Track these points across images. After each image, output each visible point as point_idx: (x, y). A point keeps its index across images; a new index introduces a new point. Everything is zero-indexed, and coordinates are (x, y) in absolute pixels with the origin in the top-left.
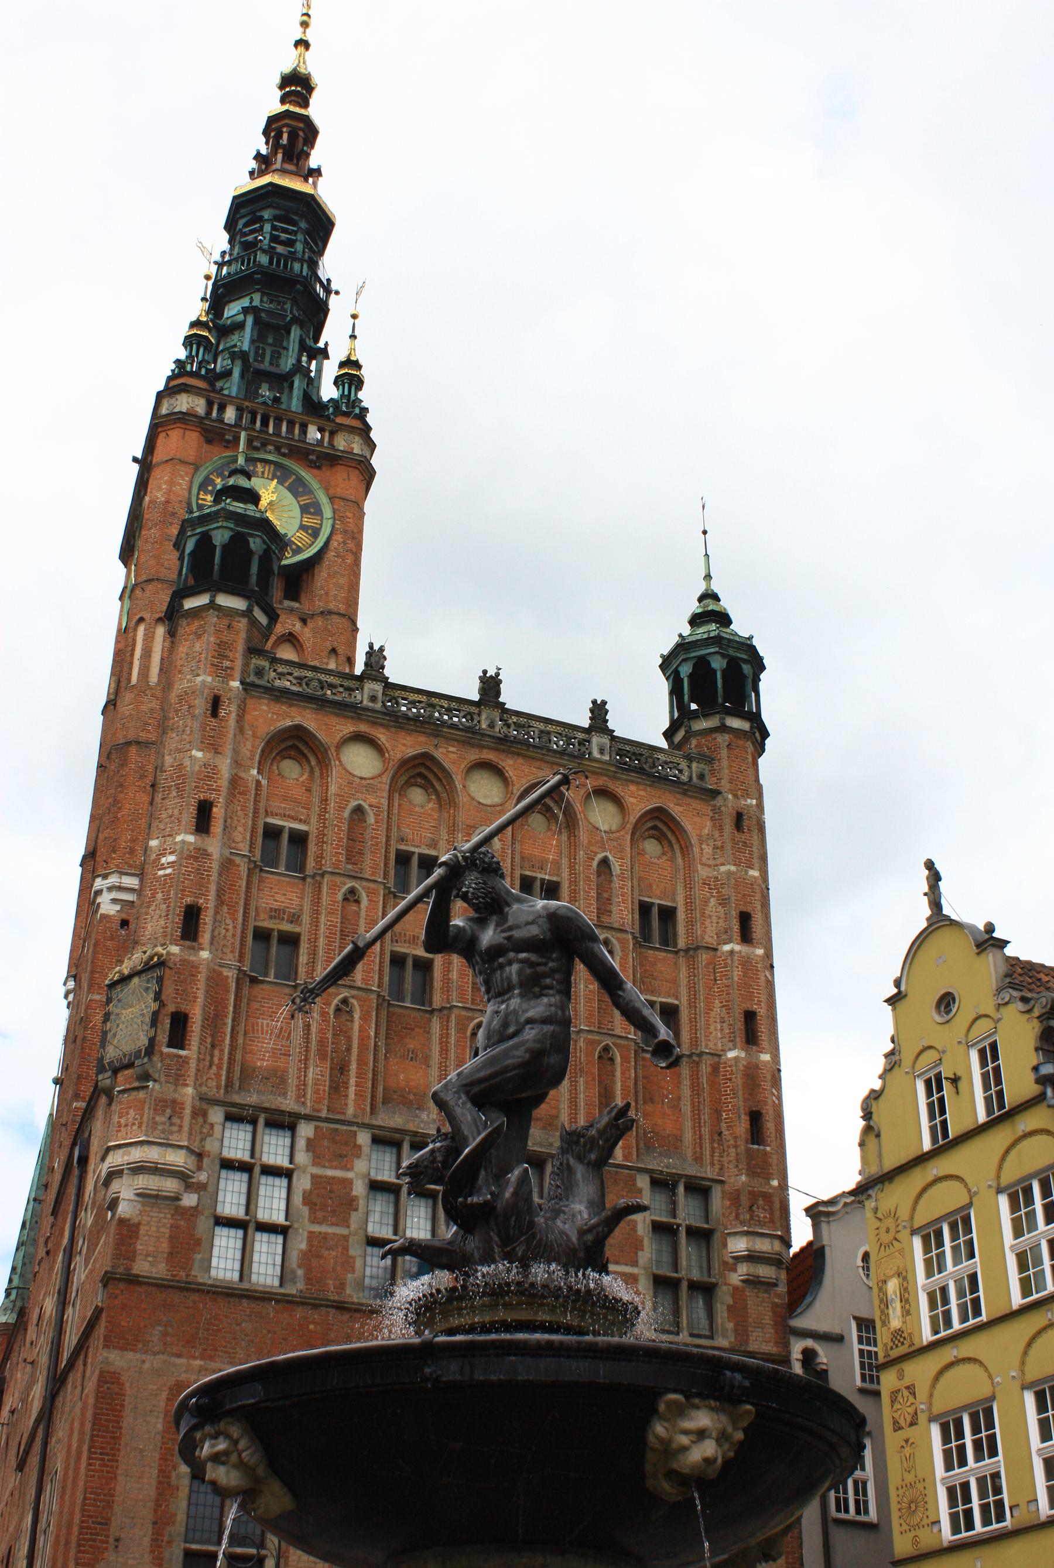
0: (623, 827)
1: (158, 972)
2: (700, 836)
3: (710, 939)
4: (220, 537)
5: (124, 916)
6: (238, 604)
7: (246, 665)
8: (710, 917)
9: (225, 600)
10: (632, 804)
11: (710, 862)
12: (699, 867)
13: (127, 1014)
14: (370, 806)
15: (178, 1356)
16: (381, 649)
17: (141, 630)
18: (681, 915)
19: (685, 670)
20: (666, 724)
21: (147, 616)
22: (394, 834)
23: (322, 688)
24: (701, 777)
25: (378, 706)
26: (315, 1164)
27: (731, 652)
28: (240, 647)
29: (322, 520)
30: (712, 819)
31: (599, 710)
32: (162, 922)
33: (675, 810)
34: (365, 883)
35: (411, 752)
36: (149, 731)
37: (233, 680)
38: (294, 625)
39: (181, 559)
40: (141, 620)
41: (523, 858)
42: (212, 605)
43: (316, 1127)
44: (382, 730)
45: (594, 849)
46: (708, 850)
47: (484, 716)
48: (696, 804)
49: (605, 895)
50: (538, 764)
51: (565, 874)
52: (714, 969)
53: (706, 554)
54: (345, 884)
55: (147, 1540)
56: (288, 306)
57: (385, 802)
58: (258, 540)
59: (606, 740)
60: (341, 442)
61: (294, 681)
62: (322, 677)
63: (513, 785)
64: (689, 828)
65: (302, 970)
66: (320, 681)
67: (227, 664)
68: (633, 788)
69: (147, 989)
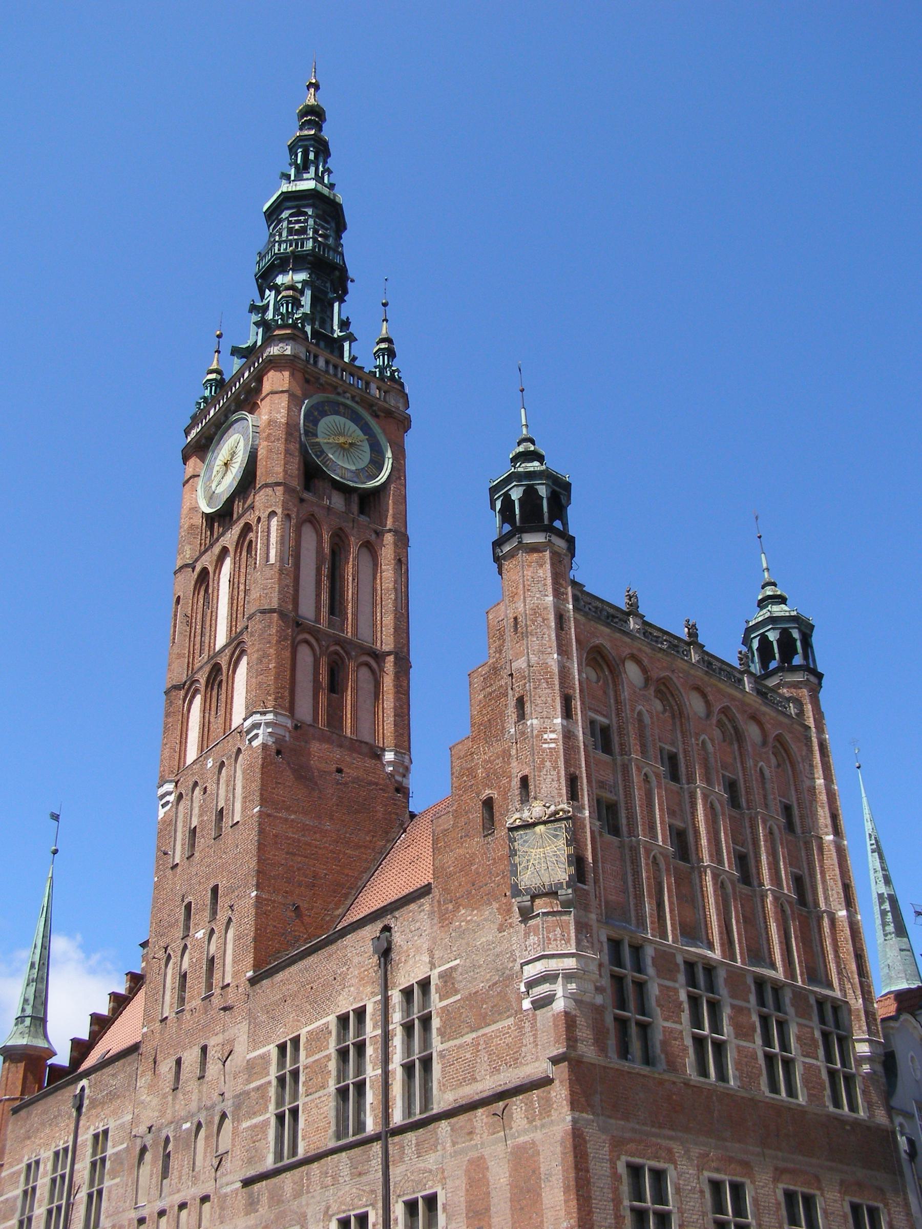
1: (563, 824)
12: (805, 779)
13: (535, 853)
15: (610, 1117)
18: (796, 811)
23: (608, 618)
26: (658, 977)
27: (803, 628)
32: (555, 784)
33: (788, 737)
34: (653, 769)
35: (663, 674)
40: (273, 513)
43: (655, 949)
51: (741, 774)
56: (328, 285)
60: (393, 401)
64: (796, 749)
65: (624, 829)
69: (556, 836)
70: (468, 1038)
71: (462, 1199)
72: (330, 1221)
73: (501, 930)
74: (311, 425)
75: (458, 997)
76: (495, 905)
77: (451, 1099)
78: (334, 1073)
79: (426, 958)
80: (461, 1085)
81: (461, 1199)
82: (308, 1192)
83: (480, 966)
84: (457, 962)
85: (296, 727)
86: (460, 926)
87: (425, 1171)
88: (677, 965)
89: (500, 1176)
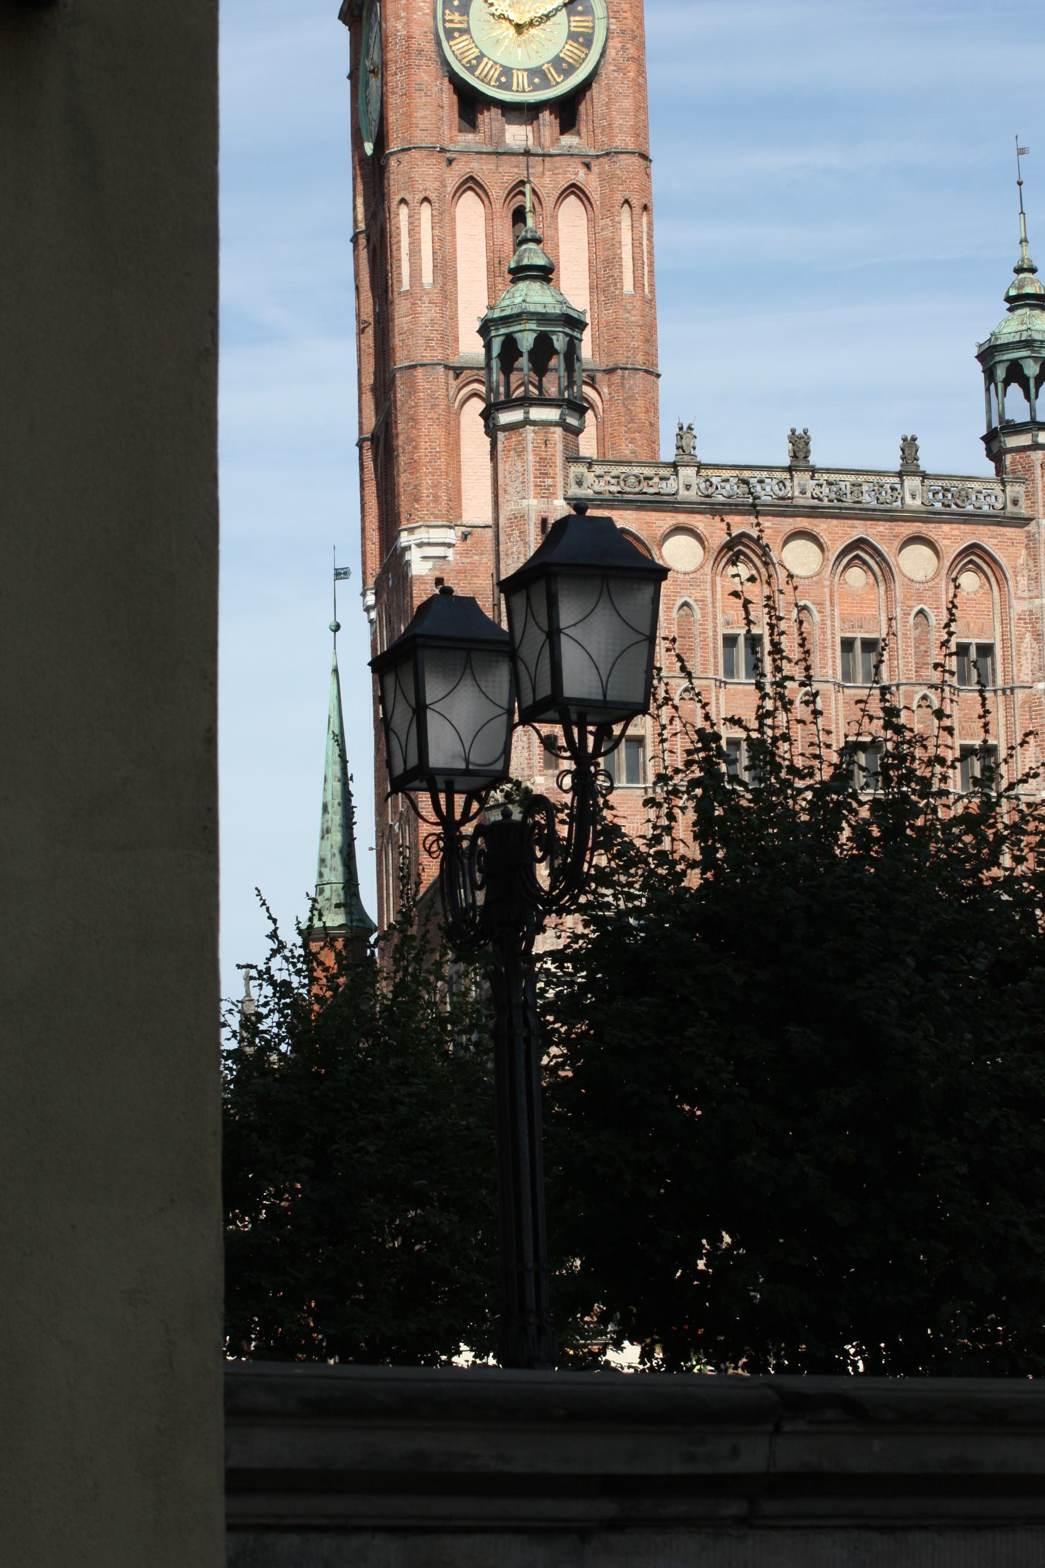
0: (937, 574)
2: (1015, 568)
3: (1025, 677)
4: (526, 341)
5: (438, 574)
6: (552, 414)
7: (566, 476)
8: (1026, 653)
9: (537, 413)
10: (946, 546)
11: (1026, 595)
14: (696, 601)
16: (690, 428)
17: (404, 211)
18: (998, 651)
19: (1001, 373)
20: (984, 432)
21: (408, 198)
22: (720, 620)
23: (639, 482)
24: (1015, 502)
25: (692, 495)
28: (559, 459)
29: (593, 22)
30: (1027, 547)
31: (909, 447)
32: (526, 754)
33: (989, 544)
36: (433, 349)
37: (556, 498)
38: (577, 174)
39: (488, 346)
40: (403, 201)
41: (843, 620)
42: (527, 422)
44: (698, 517)
45: (909, 603)
46: (1023, 581)
47: (796, 481)
48: (1009, 532)
49: (923, 648)
50: (850, 522)
52: (1030, 708)
53: (1022, 212)
54: (679, 686)
57: (709, 594)
58: (561, 335)
59: (917, 480)
61: (613, 481)
62: (636, 471)
63: (829, 550)
66: (636, 477)
67: (549, 481)
68: (946, 528)
74: (456, 17)
85: (465, 537)
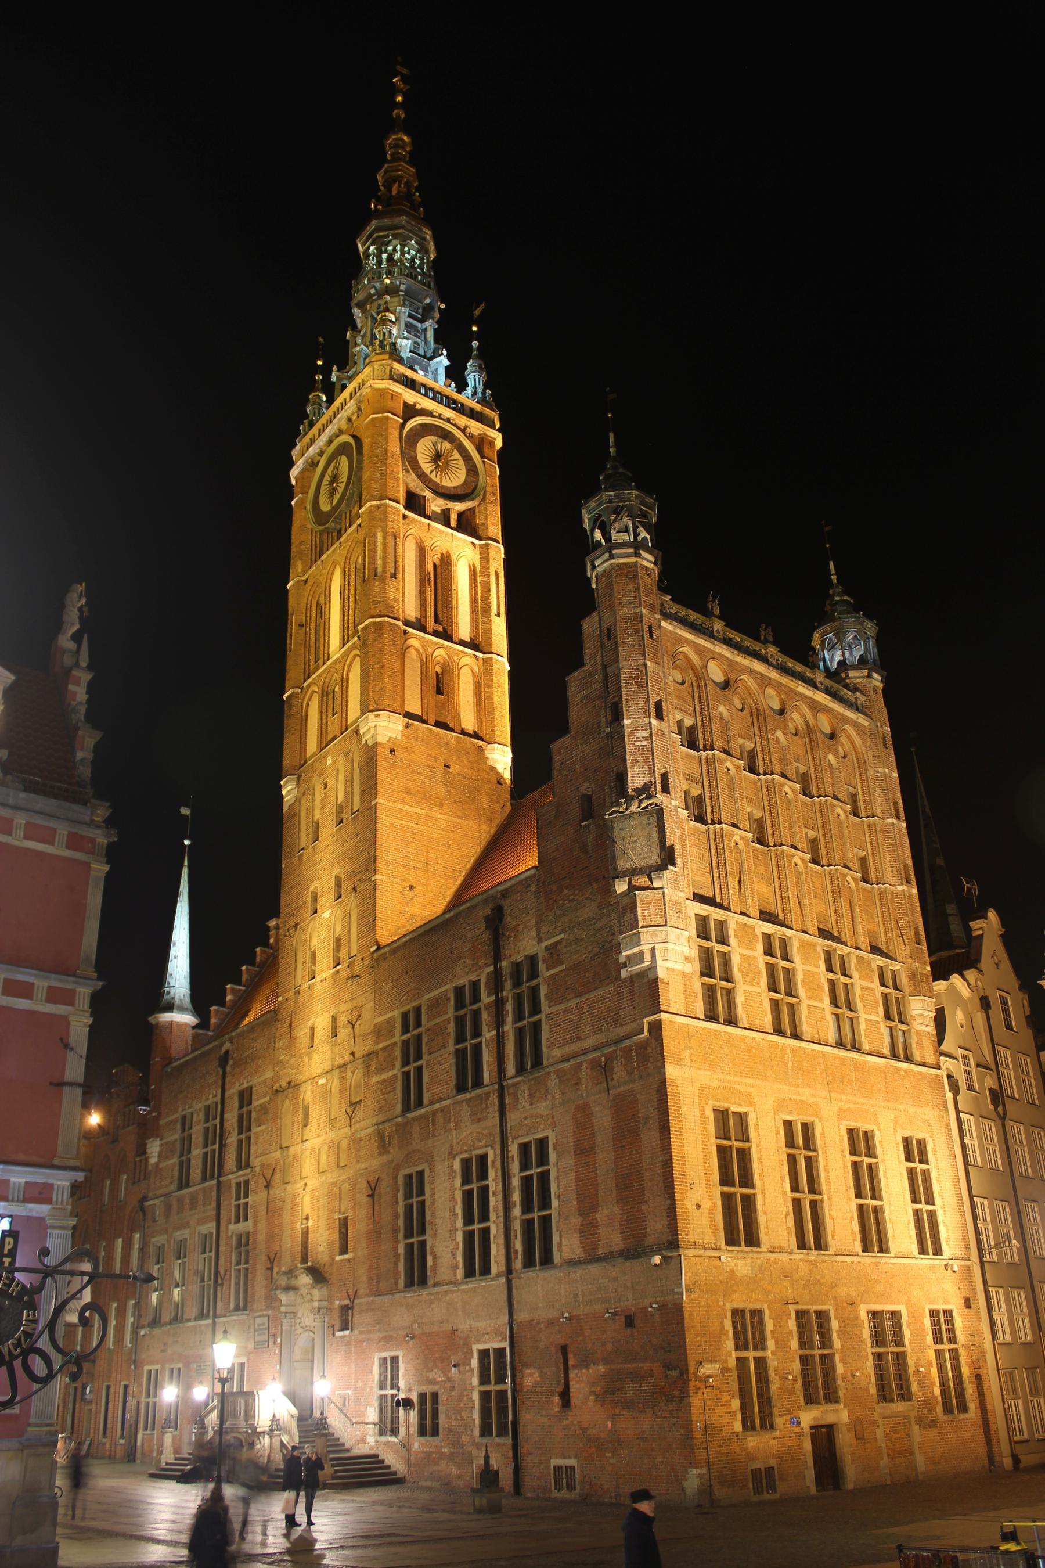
46: (871, 757)
55: (704, 1185)
70: (573, 1003)
71: (571, 1140)
72: (454, 1158)
73: (600, 907)
75: (564, 967)
76: (596, 886)
77: (559, 1055)
78: (453, 1035)
79: (533, 933)
80: (567, 1043)
81: (569, 1140)
82: (434, 1136)
83: (582, 939)
84: (562, 936)
86: (564, 904)
87: (537, 1116)
88: (756, 936)
89: (603, 1119)
